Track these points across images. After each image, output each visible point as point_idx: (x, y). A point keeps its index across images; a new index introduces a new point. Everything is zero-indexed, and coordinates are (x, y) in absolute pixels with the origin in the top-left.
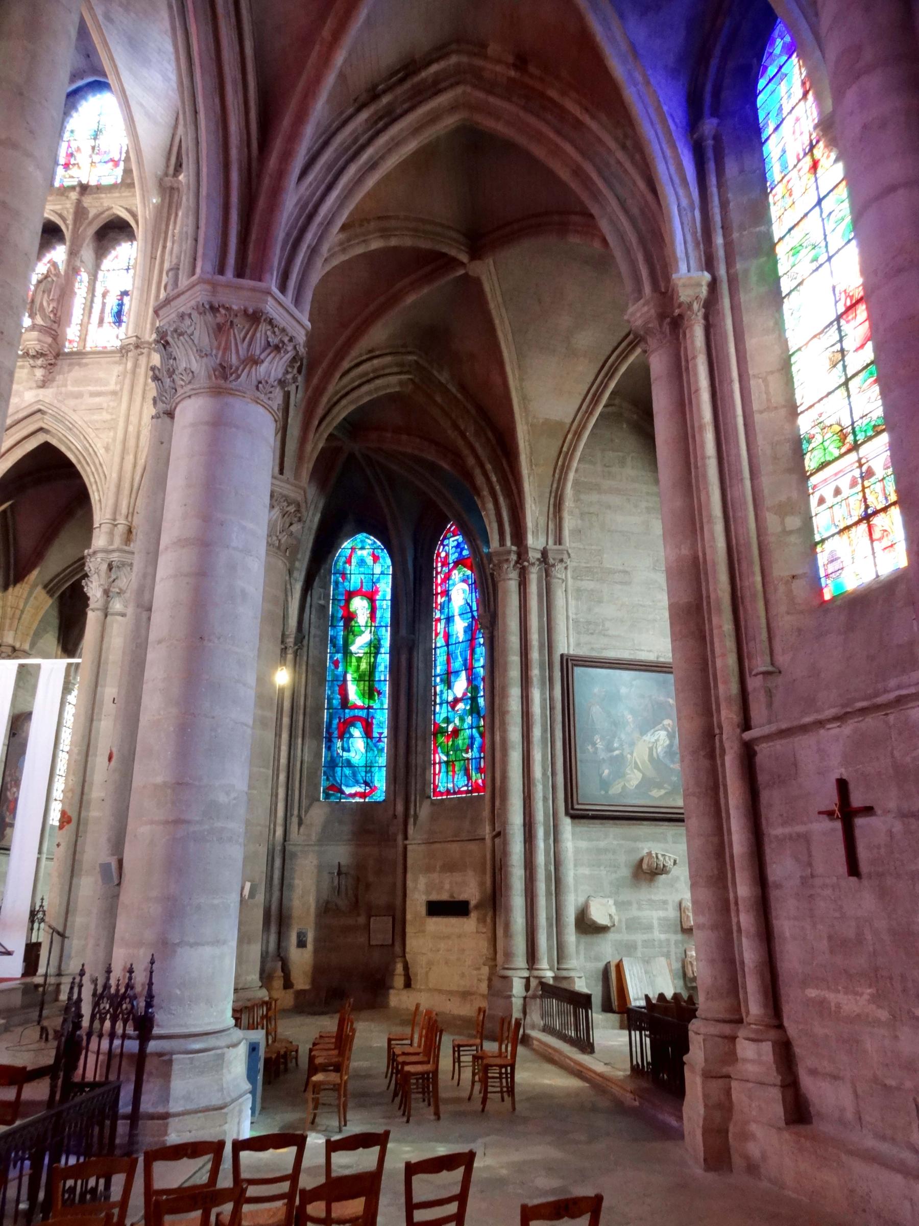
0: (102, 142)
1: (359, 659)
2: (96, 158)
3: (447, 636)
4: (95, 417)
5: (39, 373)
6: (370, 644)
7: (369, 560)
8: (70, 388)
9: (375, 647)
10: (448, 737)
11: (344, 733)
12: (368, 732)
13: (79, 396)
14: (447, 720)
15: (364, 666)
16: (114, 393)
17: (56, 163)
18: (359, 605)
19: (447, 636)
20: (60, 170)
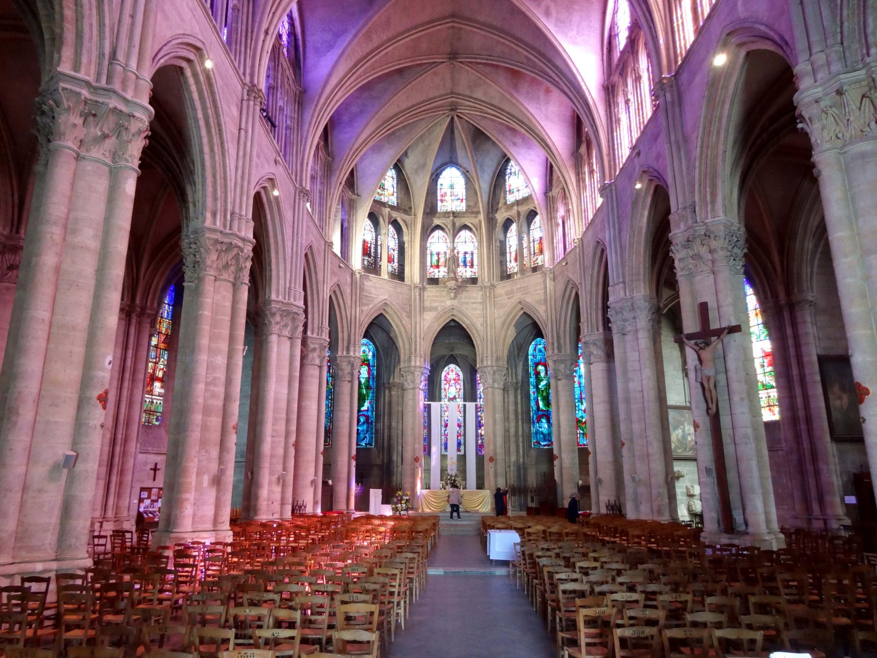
0: (455, 191)
1: (543, 391)
2: (453, 198)
3: (579, 383)
4: (475, 312)
5: (452, 295)
6: (546, 384)
7: (543, 350)
8: (463, 300)
9: (548, 386)
10: (583, 423)
11: (539, 421)
12: (548, 421)
13: (467, 303)
14: (582, 417)
15: (544, 394)
16: (480, 303)
17: (437, 200)
18: (541, 368)
19: (579, 383)
20: (439, 203)
